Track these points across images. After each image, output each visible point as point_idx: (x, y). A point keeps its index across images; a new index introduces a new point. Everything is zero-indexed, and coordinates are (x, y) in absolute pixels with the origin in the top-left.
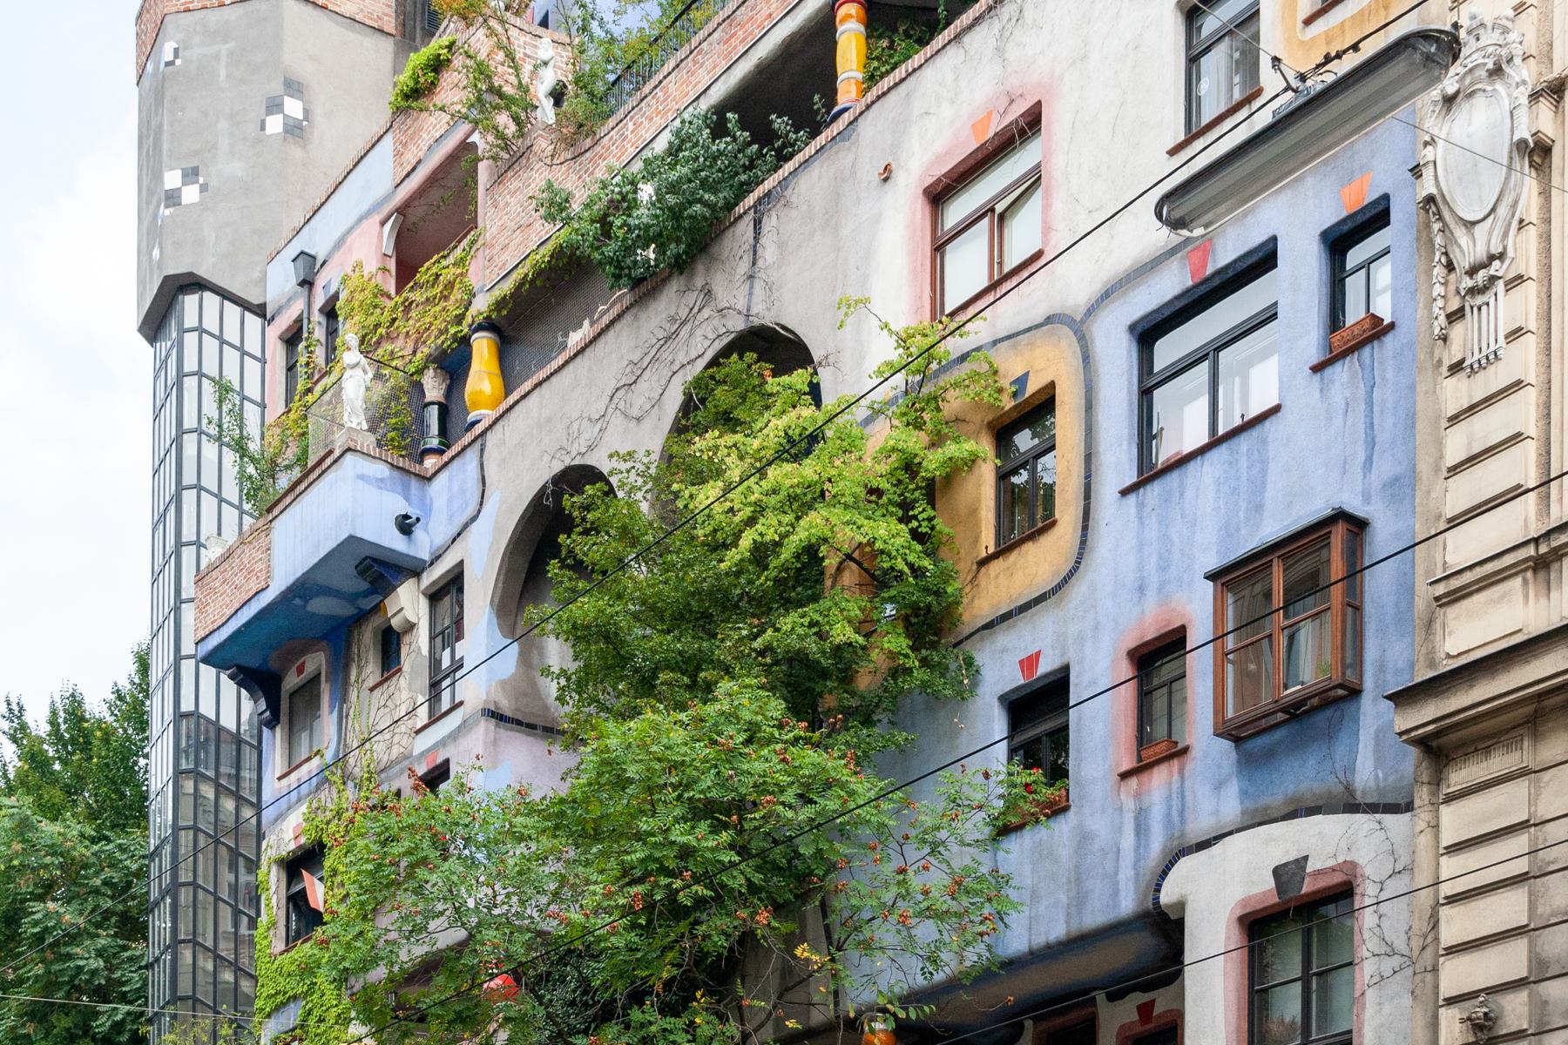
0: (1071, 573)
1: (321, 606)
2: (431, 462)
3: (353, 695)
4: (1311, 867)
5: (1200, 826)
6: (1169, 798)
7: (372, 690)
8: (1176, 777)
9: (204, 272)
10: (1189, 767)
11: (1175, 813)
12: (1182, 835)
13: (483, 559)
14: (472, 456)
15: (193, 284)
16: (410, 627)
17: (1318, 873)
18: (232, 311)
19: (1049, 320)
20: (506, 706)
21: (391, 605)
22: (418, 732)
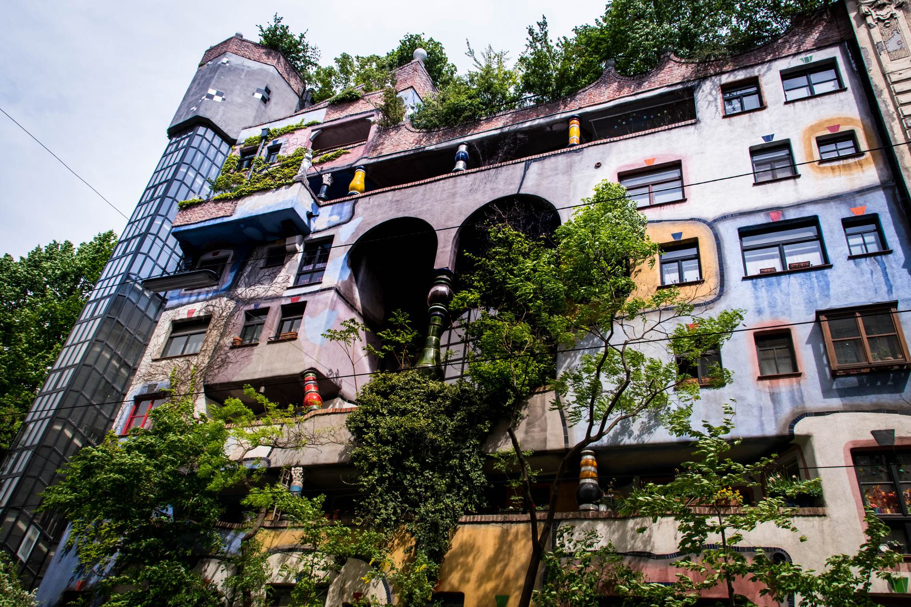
0: (713, 301)
1: (251, 231)
2: (322, 202)
3: (249, 269)
4: (896, 435)
5: (810, 406)
6: (792, 391)
7: (261, 268)
8: (795, 384)
9: (216, 120)
10: (802, 382)
11: (797, 397)
12: (804, 407)
13: (346, 236)
14: (347, 207)
15: (208, 124)
16: (295, 252)
17: (901, 438)
18: (217, 141)
19: (691, 219)
20: (342, 290)
21: (289, 241)
22: (288, 288)
